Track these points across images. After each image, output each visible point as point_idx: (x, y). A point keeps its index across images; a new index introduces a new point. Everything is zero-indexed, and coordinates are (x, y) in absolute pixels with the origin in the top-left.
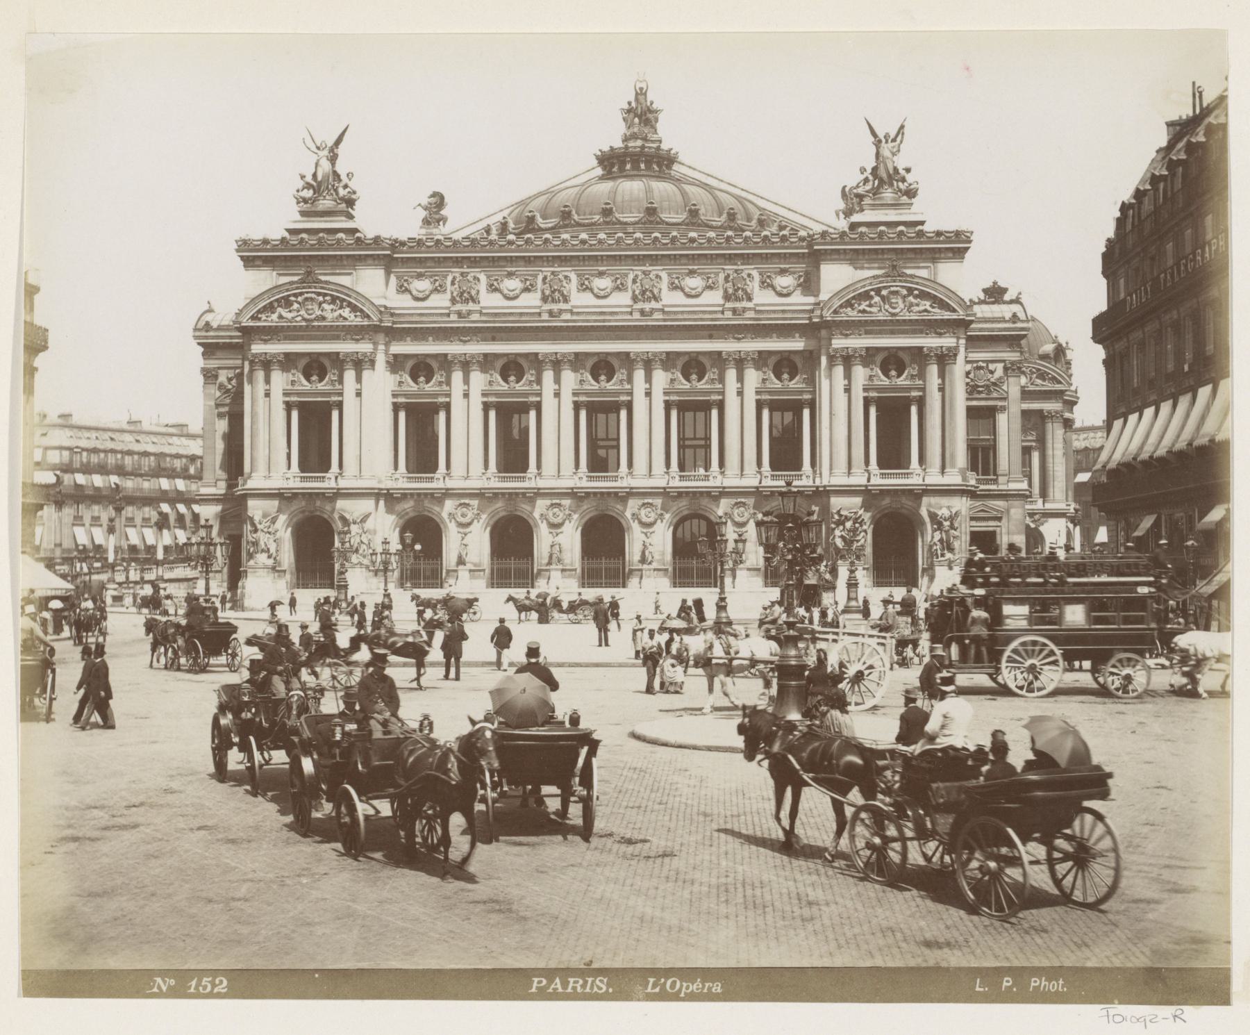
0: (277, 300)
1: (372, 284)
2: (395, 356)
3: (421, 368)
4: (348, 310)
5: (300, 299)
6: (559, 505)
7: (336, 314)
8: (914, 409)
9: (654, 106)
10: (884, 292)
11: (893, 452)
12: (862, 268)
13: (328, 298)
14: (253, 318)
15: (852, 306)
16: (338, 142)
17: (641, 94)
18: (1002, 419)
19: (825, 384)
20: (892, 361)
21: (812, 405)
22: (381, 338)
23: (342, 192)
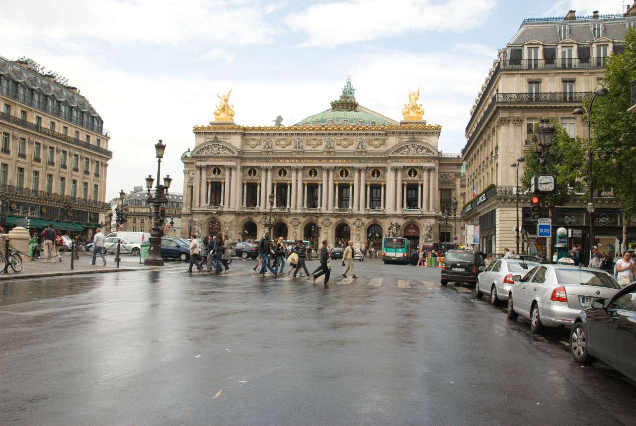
1: (236, 142)
2: (244, 167)
3: (253, 171)
8: (420, 188)
9: (354, 88)
10: (409, 147)
11: (412, 202)
12: (403, 139)
13: (221, 147)
15: (398, 152)
16: (229, 94)
17: (349, 83)
18: (453, 192)
19: (388, 179)
20: (413, 171)
21: (385, 186)
22: (239, 161)
23: (229, 112)
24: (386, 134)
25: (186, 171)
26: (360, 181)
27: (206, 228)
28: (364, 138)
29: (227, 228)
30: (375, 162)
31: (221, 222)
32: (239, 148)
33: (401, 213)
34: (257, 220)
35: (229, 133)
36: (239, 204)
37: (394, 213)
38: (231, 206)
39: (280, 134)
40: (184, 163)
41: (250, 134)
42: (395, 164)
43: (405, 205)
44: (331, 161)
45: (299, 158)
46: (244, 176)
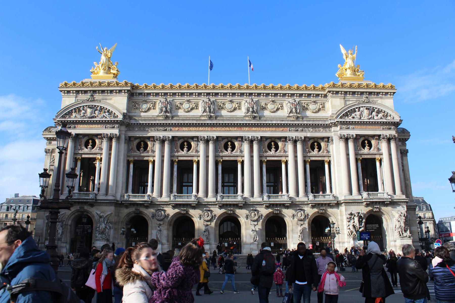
0: (75, 109)
2: (130, 137)
4: (107, 114)
6: (209, 210)
7: (102, 115)
10: (361, 109)
12: (349, 100)
13: (98, 108)
14: (63, 117)
15: (347, 115)
21: (329, 163)
22: (123, 128)
24: (326, 96)
25: (49, 150)
26: (296, 157)
27: (71, 226)
28: (298, 99)
29: (103, 226)
30: (316, 131)
31: (94, 216)
32: (125, 111)
33: (360, 197)
34: (148, 214)
35: (111, 91)
36: (122, 189)
37: (351, 197)
38: (110, 192)
39: (183, 94)
40: (47, 139)
41: (141, 94)
42: (346, 132)
43: (362, 188)
44: (254, 129)
45: (211, 124)
46: (129, 150)
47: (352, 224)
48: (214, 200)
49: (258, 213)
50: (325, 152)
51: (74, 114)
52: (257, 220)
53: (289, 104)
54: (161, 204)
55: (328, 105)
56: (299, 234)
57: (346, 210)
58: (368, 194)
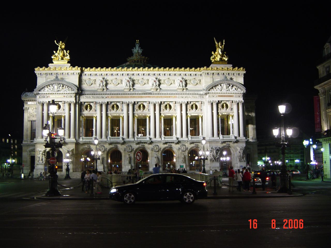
2: (81, 102)
4: (67, 88)
5: (53, 85)
10: (222, 85)
21: (202, 117)
30: (194, 97)
42: (212, 99)
47: (212, 154)
48: (133, 140)
49: (158, 147)
50: (200, 110)
51: (46, 89)
52: (158, 151)
53: (178, 81)
54: (102, 143)
55: (203, 81)
56: (182, 159)
57: (210, 146)
58: (223, 137)
